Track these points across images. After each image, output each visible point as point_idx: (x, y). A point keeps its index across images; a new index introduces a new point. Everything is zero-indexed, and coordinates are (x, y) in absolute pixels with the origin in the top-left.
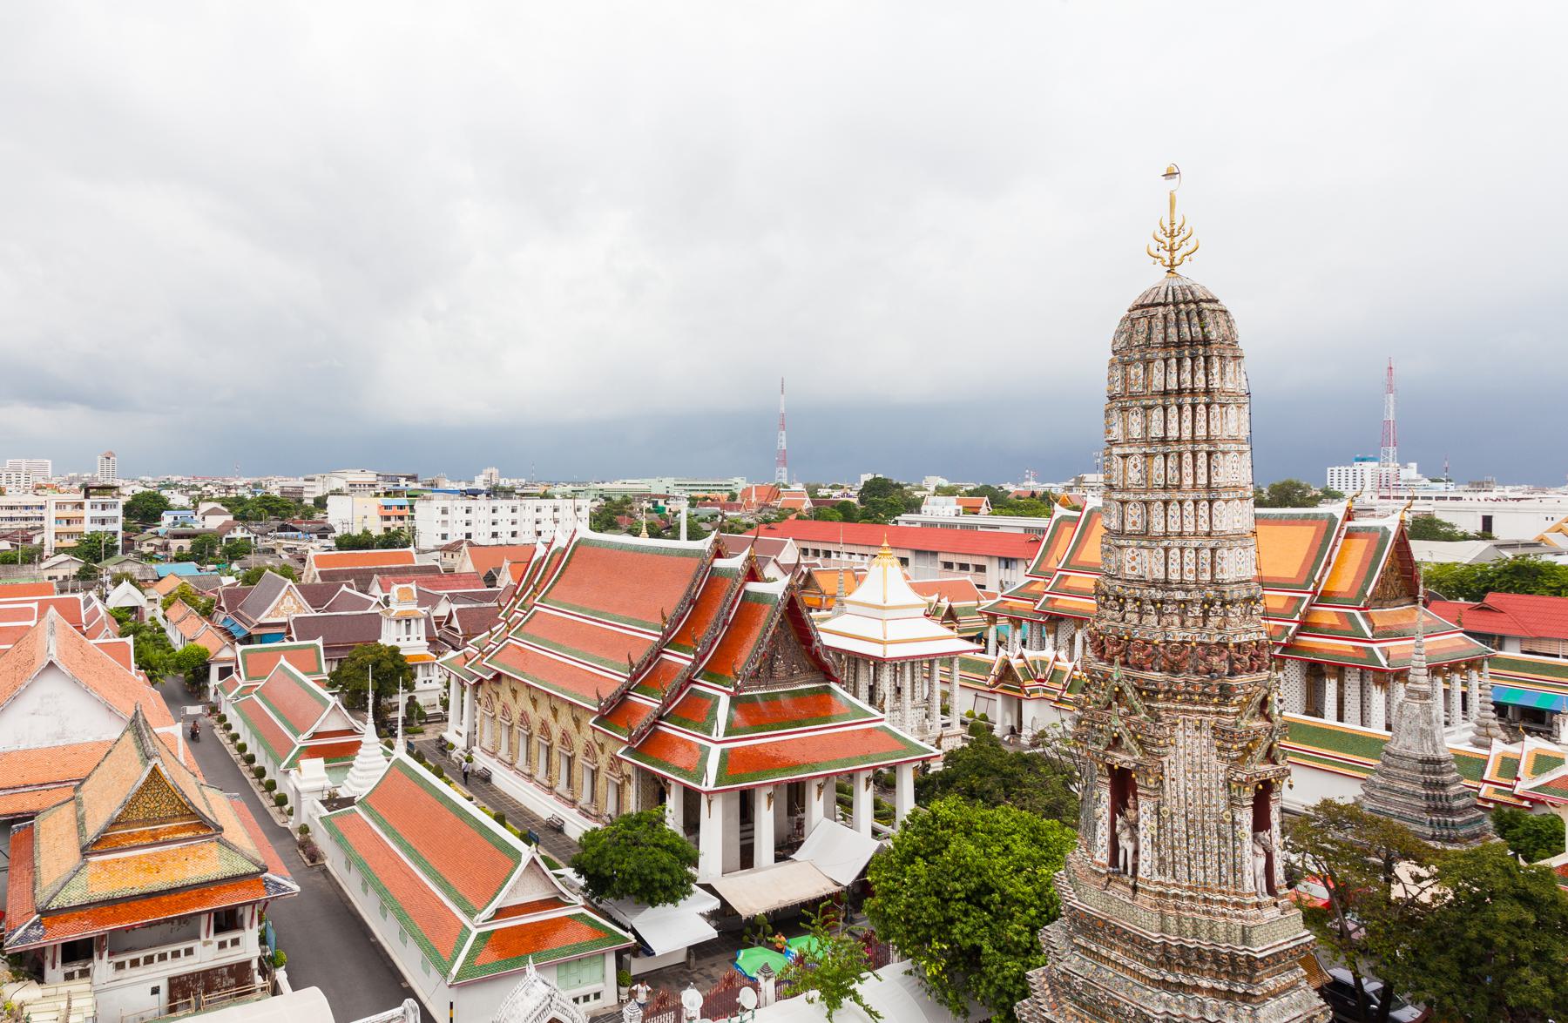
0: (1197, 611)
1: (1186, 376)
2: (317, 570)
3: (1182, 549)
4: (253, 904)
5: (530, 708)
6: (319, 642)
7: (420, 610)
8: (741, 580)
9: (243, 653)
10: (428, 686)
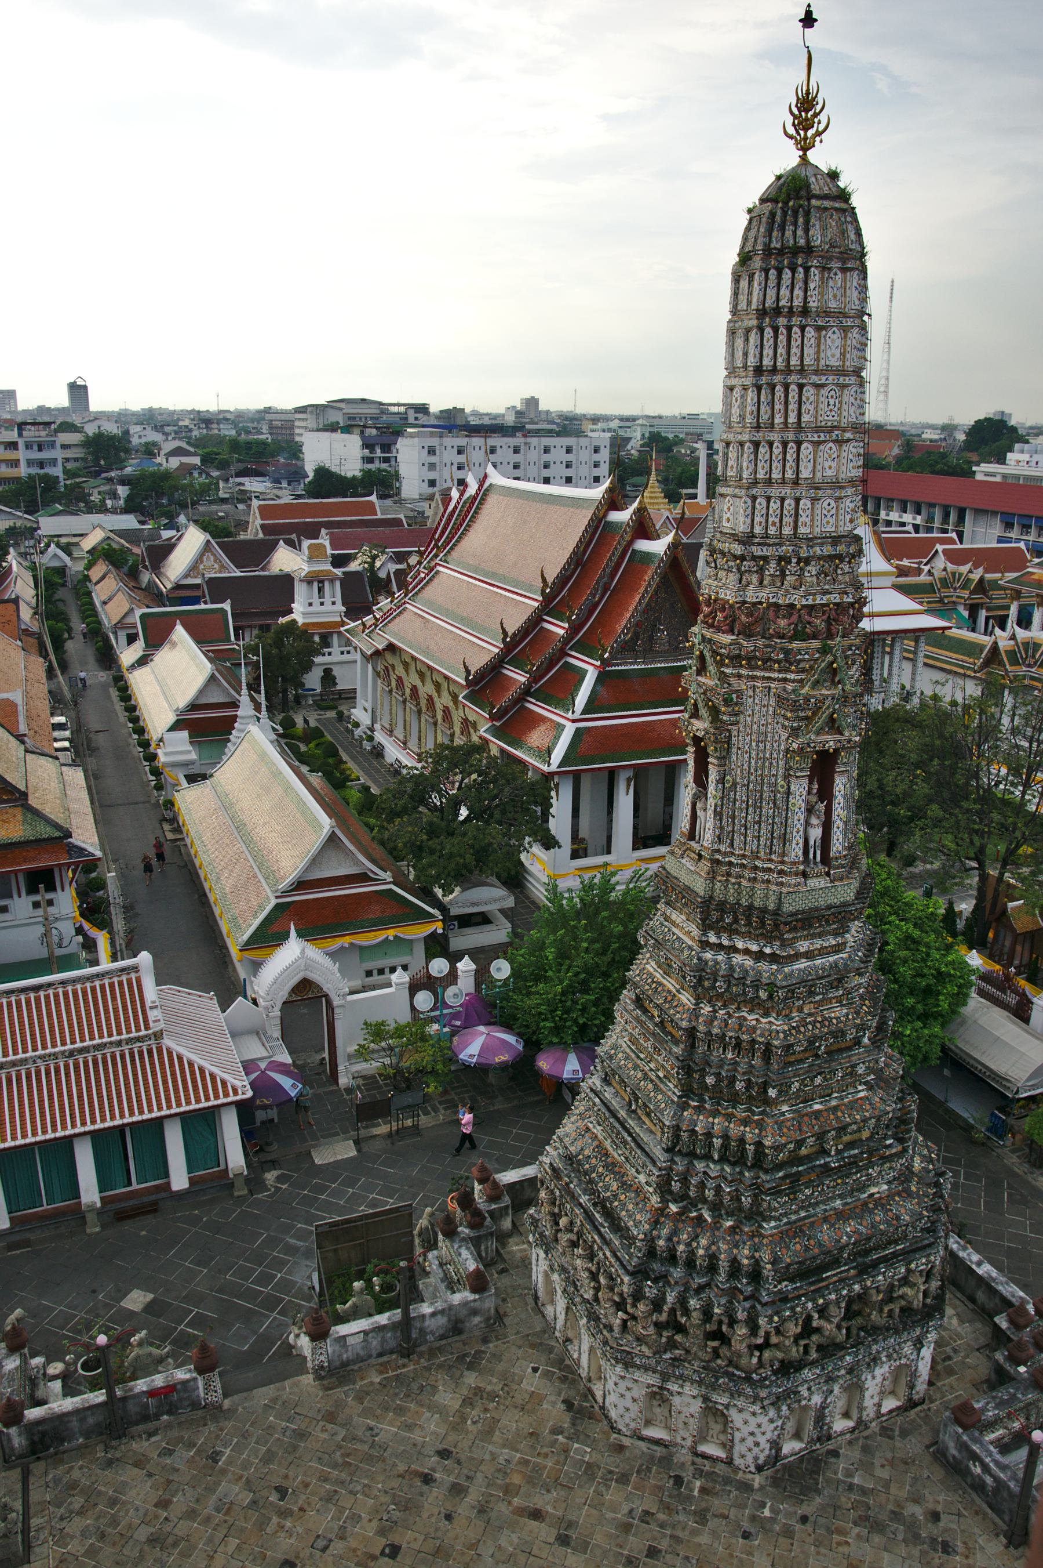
0: (772, 568)
1: (784, 292)
2: (259, 522)
3: (768, 499)
4: (69, 865)
5: (418, 683)
6: (227, 606)
7: (335, 571)
8: (627, 537)
9: (143, 617)
10: (346, 657)
